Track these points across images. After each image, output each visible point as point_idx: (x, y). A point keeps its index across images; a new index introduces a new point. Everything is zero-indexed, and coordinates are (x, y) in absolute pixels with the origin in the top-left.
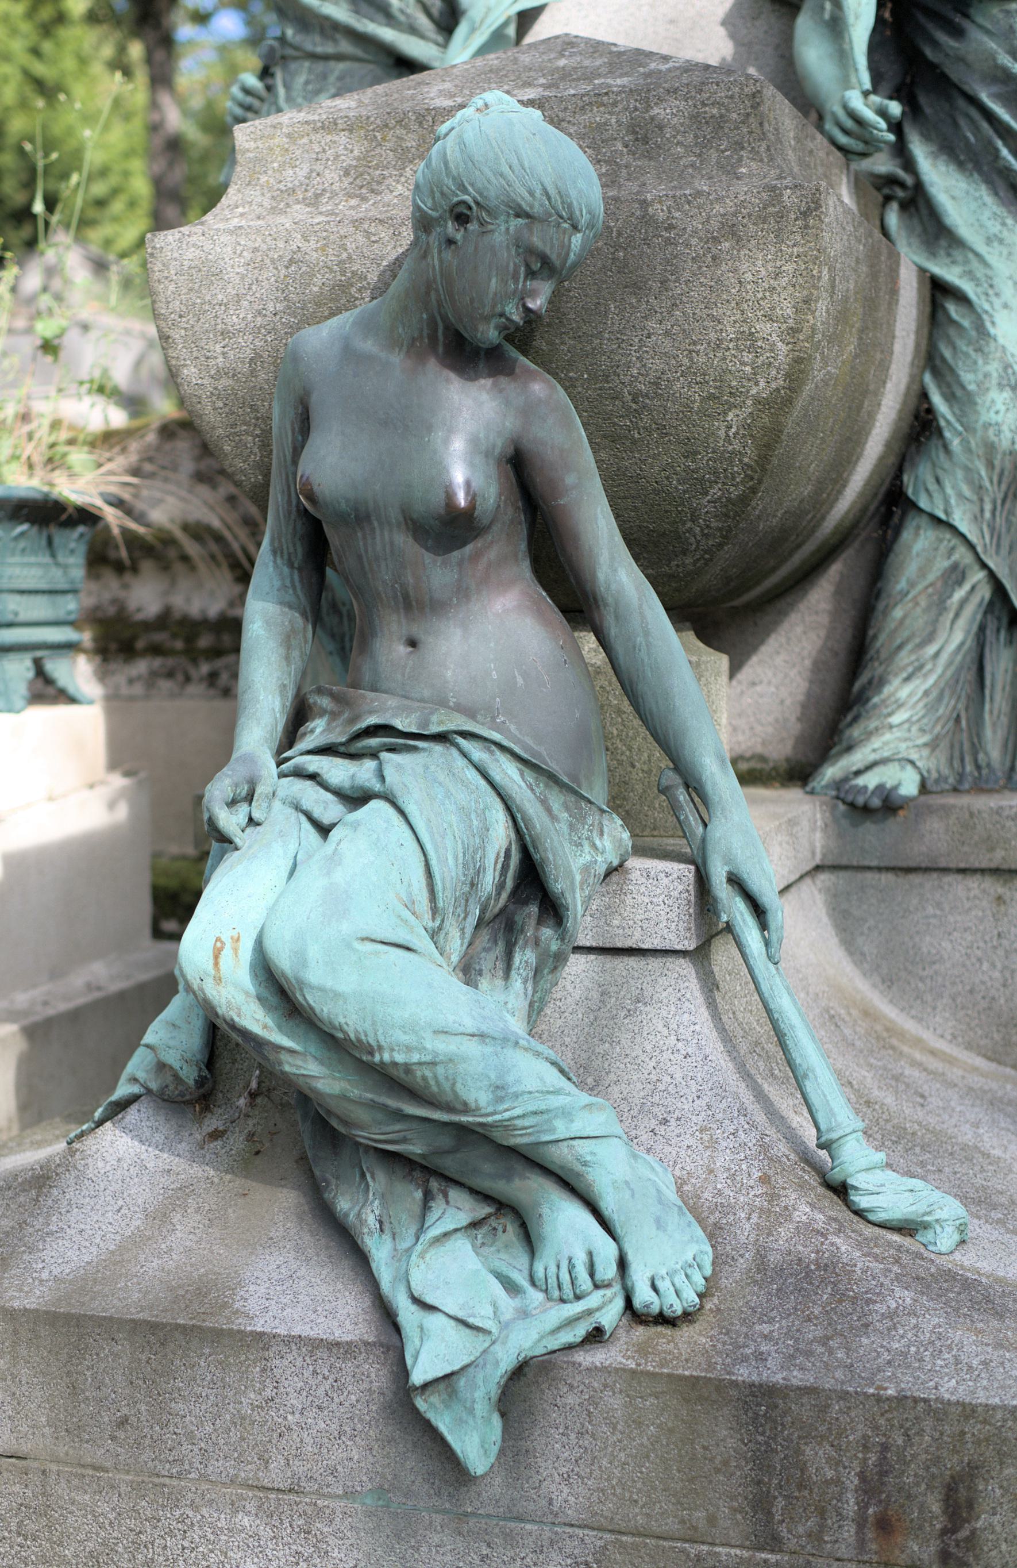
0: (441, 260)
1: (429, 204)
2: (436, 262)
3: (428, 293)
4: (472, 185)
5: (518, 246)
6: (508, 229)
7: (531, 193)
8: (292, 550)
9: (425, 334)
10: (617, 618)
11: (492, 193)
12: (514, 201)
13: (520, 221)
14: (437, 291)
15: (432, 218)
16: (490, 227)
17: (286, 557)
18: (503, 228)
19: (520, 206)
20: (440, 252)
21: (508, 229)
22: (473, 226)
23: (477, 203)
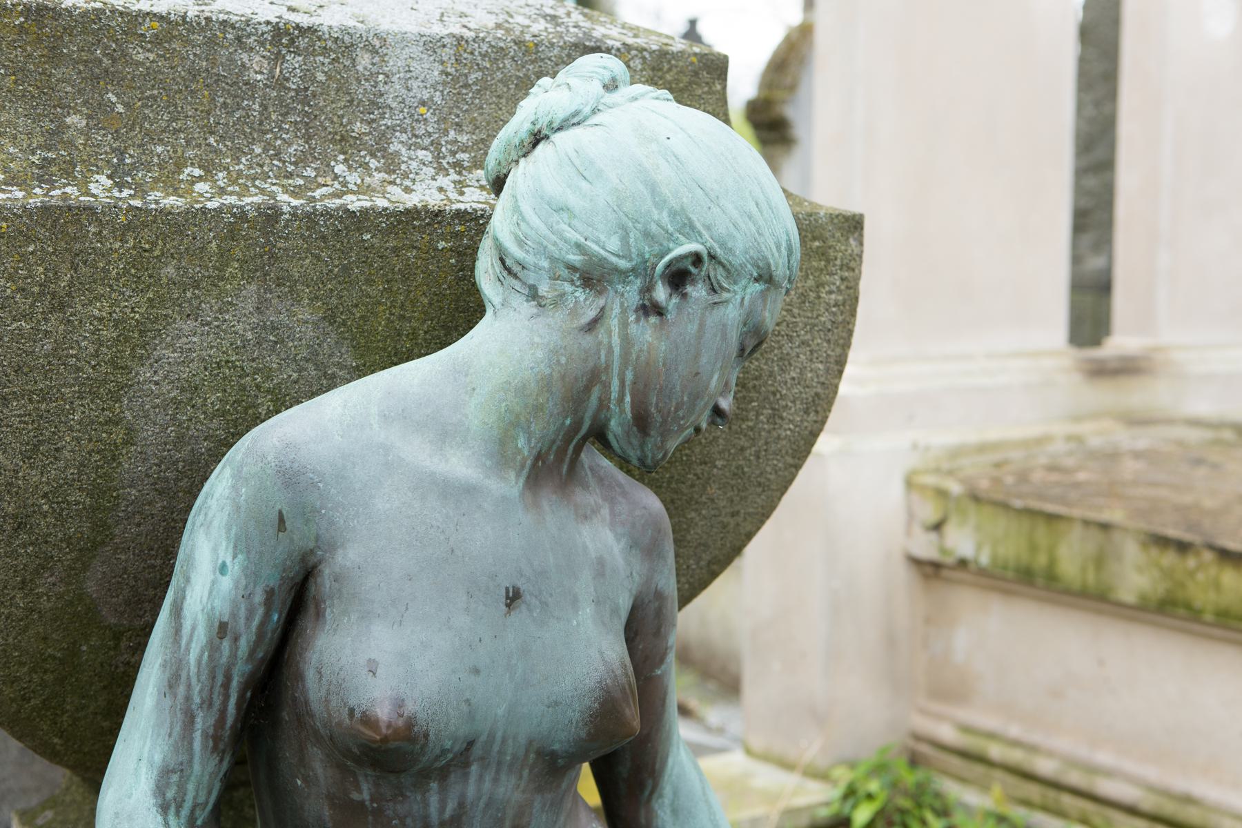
0: (626, 341)
1: (614, 244)
2: (616, 340)
3: (587, 389)
4: (708, 228)
5: (745, 325)
6: (743, 299)
7: (778, 247)
8: (201, 799)
9: (554, 448)
10: (675, 812)
11: (739, 245)
12: (765, 258)
13: (758, 287)
14: (607, 386)
15: (616, 270)
16: (725, 295)
17: (185, 812)
18: (738, 297)
19: (769, 265)
20: (624, 325)
21: (743, 299)
22: (698, 291)
23: (712, 257)
